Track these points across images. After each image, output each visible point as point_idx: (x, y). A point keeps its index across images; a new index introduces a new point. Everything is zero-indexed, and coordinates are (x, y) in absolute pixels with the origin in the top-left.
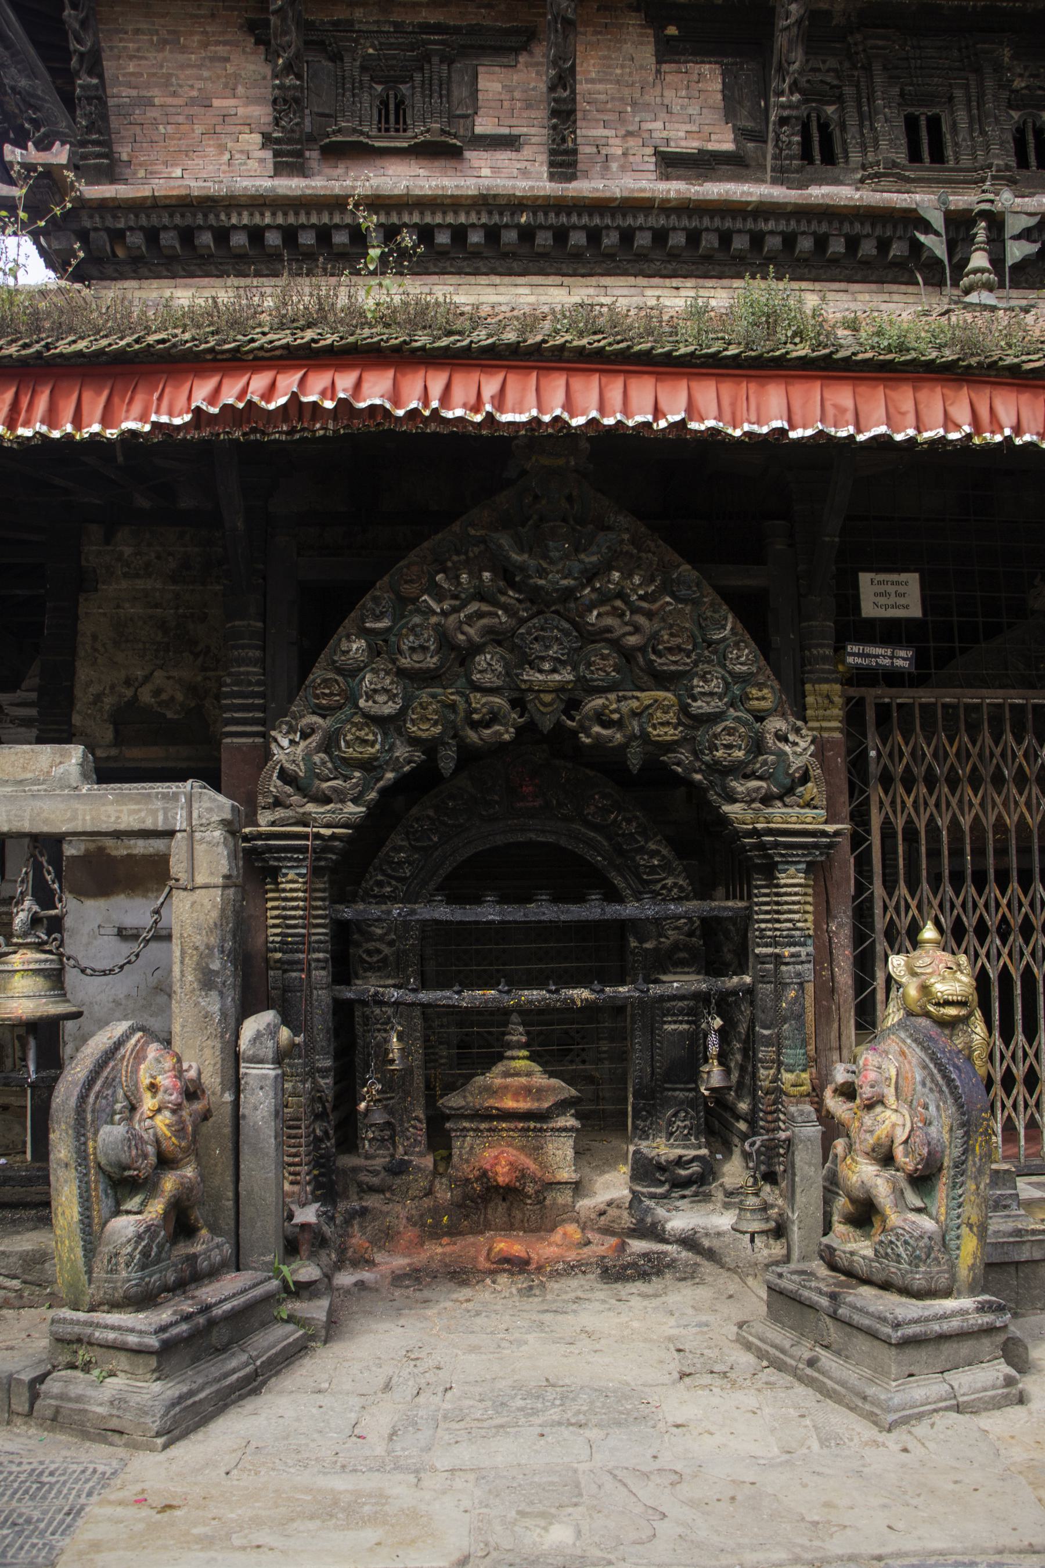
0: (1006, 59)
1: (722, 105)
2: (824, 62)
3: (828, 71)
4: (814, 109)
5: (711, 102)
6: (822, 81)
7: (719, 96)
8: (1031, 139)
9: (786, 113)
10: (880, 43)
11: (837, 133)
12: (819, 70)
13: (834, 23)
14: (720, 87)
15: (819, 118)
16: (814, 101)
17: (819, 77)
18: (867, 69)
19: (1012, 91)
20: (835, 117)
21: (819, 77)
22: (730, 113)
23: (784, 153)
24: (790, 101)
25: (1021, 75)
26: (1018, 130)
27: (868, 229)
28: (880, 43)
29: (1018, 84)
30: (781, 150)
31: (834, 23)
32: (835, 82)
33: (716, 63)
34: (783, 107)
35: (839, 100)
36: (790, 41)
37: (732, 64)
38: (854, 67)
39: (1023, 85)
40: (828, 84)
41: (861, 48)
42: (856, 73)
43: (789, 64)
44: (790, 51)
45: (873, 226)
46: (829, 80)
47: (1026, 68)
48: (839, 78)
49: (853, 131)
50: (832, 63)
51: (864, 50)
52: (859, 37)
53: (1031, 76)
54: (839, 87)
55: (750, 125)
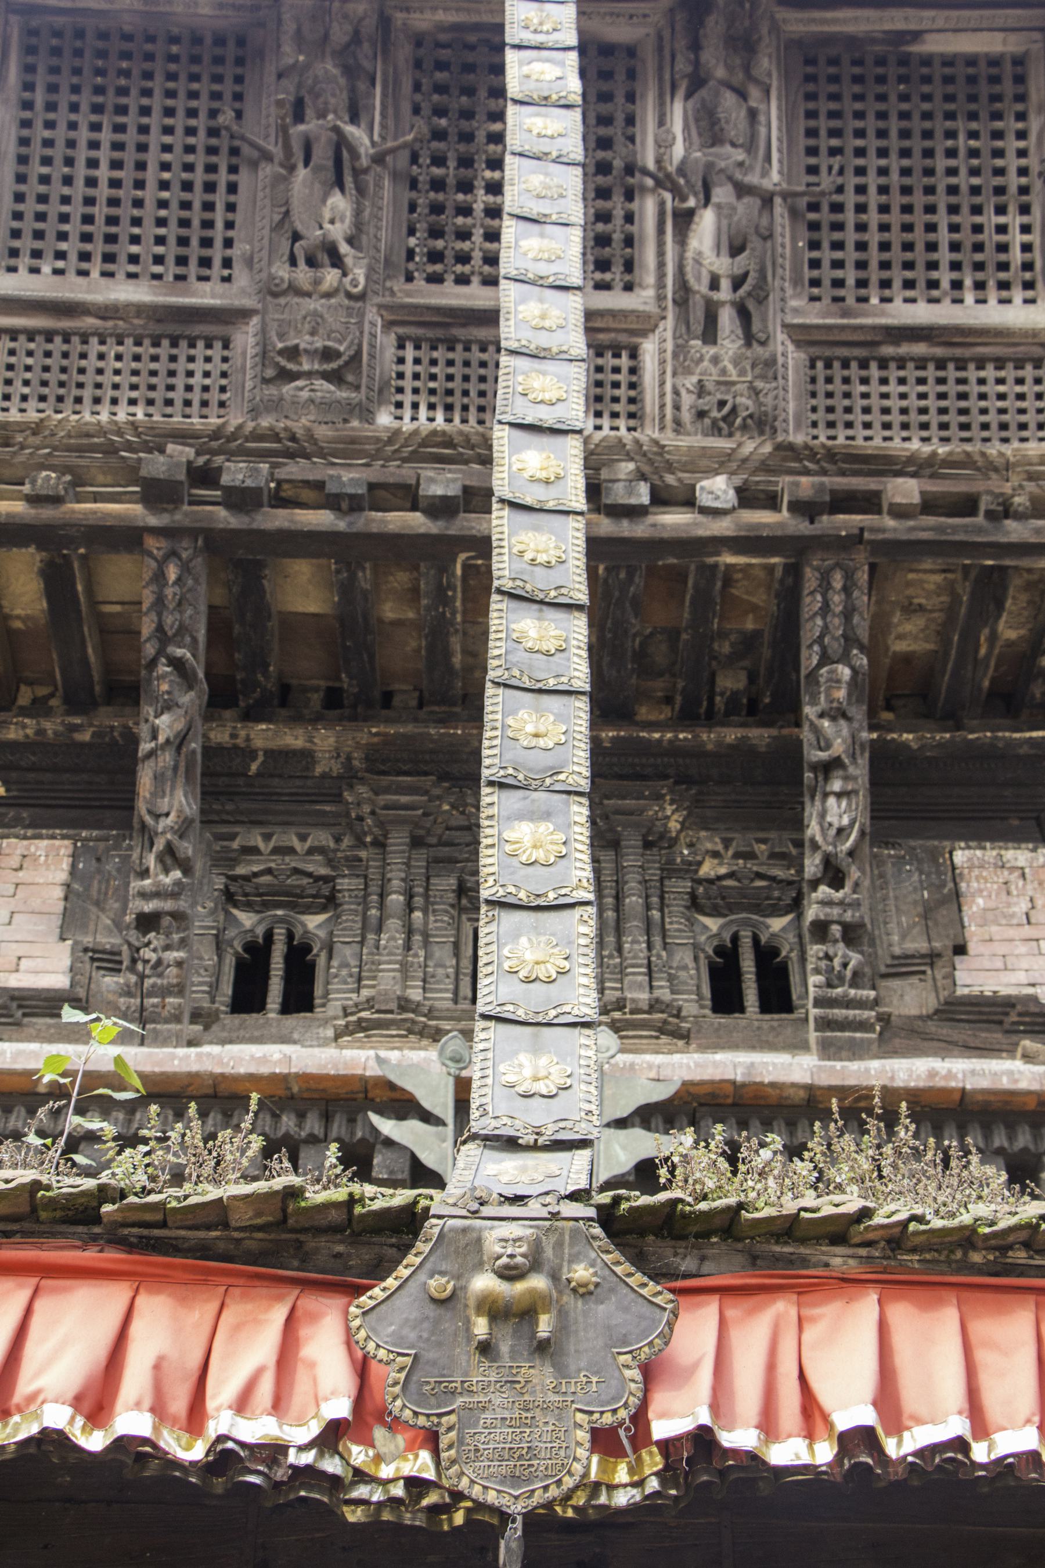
0: (674, 825)
1: (60, 905)
2: (303, 838)
3: (311, 851)
4: (281, 920)
5: (36, 904)
6: (296, 871)
7: (59, 893)
8: (748, 965)
9: (149, 907)
10: (404, 799)
11: (321, 961)
12: (291, 851)
13: (318, 770)
14: (62, 876)
15: (290, 936)
16: (278, 905)
17: (292, 862)
18: (380, 844)
19: (699, 882)
20: (322, 934)
21: (292, 862)
22: (71, 921)
23: (148, 982)
24: (157, 884)
25: (716, 855)
26: (719, 951)
27: (313, 1125)
28: (404, 799)
29: (708, 869)
30: (142, 977)
31: (318, 770)
32: (323, 871)
33: (64, 837)
34: (143, 895)
35: (330, 902)
36: (158, 778)
37: (98, 839)
38: (360, 843)
39: (723, 871)
40: (310, 875)
41: (367, 809)
42: (363, 854)
43: (157, 817)
44: (158, 792)
45: (327, 1118)
46: (310, 868)
47: (727, 843)
48: (330, 863)
49: (346, 953)
50: (322, 837)
51: (373, 813)
52: (363, 790)
53: (737, 855)
54: (326, 879)
55: (108, 940)
